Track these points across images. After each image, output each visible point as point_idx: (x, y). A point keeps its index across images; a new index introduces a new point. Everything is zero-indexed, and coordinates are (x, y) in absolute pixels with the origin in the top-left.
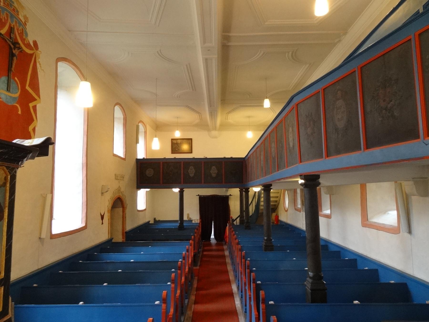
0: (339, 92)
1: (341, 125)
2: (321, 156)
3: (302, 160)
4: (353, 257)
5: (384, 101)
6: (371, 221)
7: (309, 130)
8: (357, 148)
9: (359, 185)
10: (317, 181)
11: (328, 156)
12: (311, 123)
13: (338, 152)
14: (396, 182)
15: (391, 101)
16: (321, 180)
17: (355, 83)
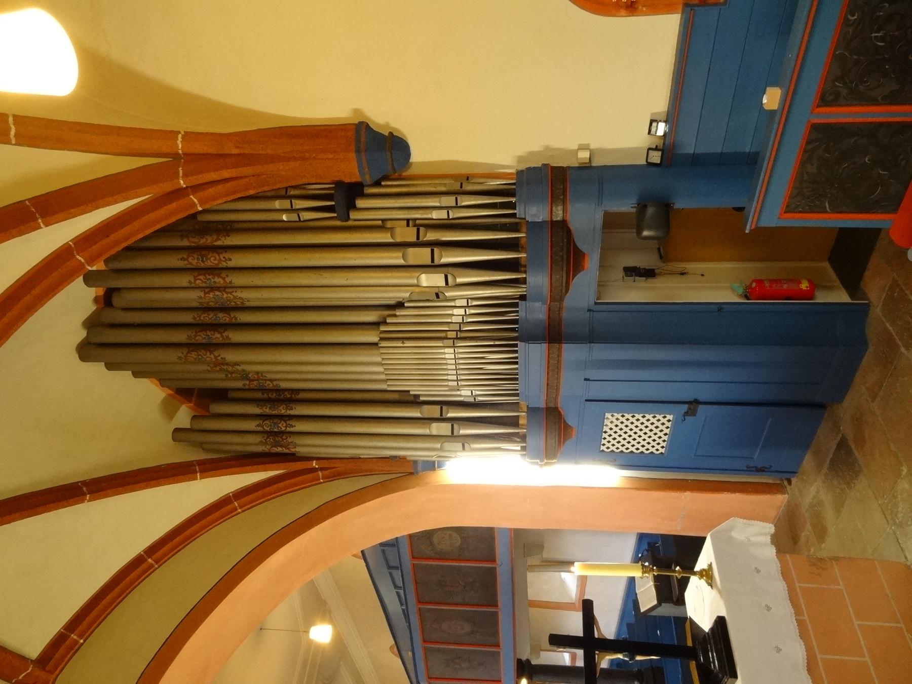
0: (433, 626)
1: (467, 628)
2: (498, 654)
3: (498, 679)
4: (625, 629)
5: (457, 587)
6: (574, 600)
7: (465, 665)
8: (495, 616)
9: (530, 608)
10: (524, 663)
11: (498, 646)
12: (457, 661)
13: (496, 634)
14: (527, 569)
15: (459, 582)
16: (524, 658)
17: (430, 610)
